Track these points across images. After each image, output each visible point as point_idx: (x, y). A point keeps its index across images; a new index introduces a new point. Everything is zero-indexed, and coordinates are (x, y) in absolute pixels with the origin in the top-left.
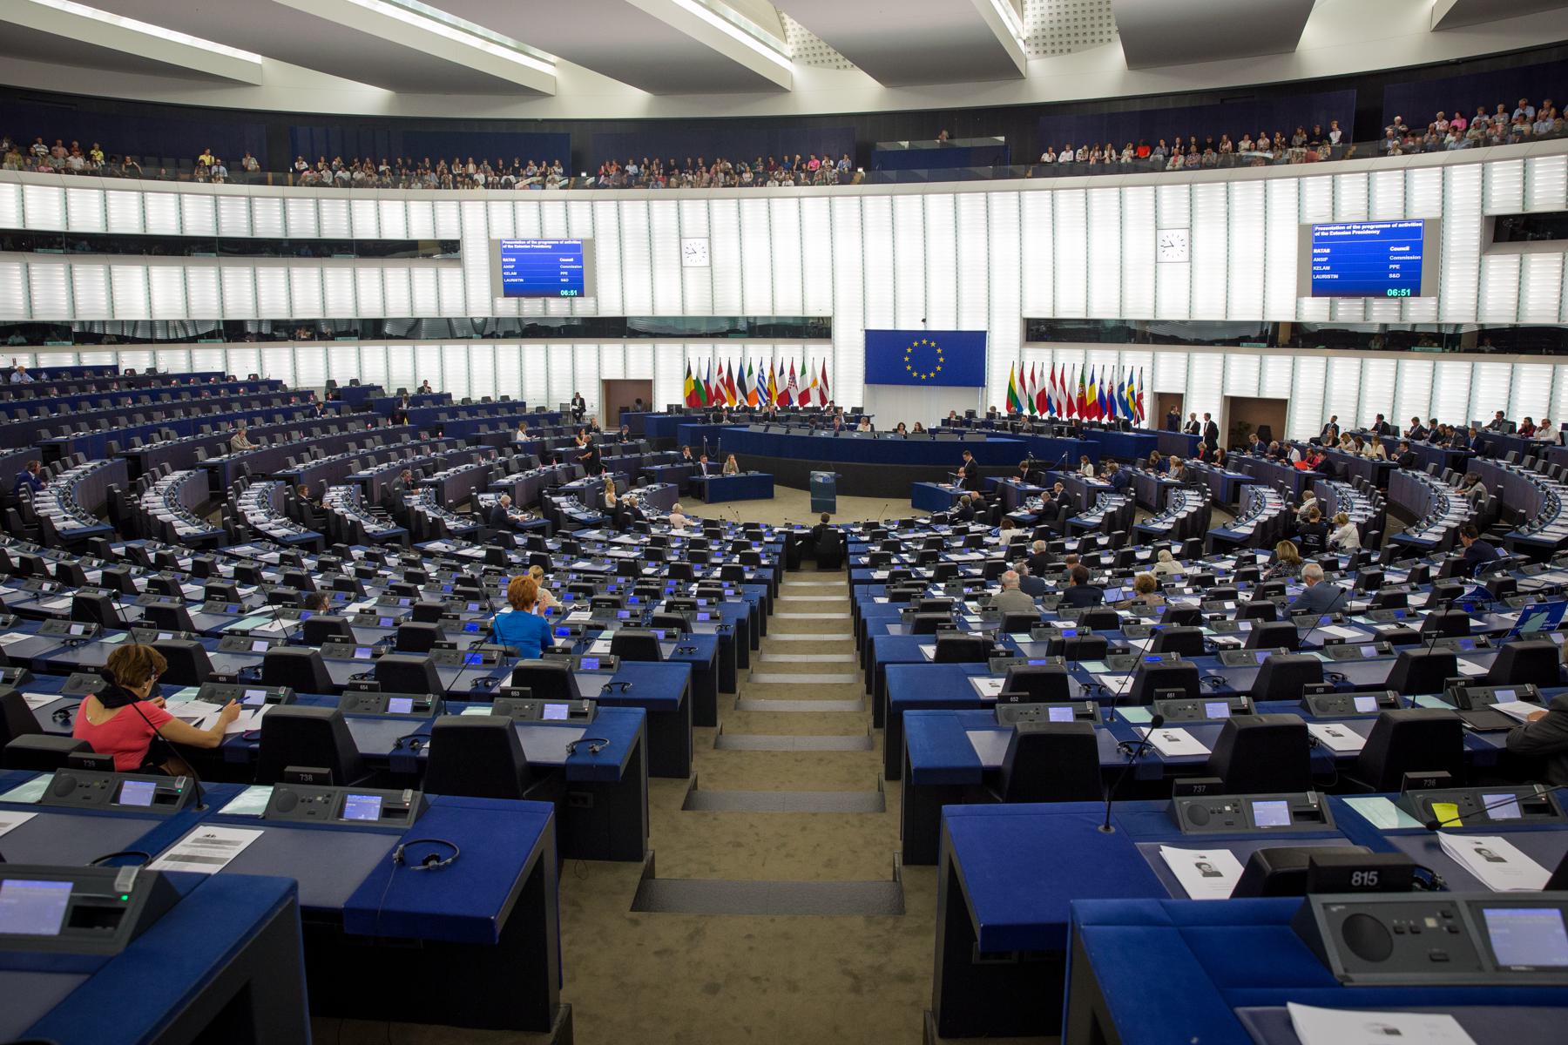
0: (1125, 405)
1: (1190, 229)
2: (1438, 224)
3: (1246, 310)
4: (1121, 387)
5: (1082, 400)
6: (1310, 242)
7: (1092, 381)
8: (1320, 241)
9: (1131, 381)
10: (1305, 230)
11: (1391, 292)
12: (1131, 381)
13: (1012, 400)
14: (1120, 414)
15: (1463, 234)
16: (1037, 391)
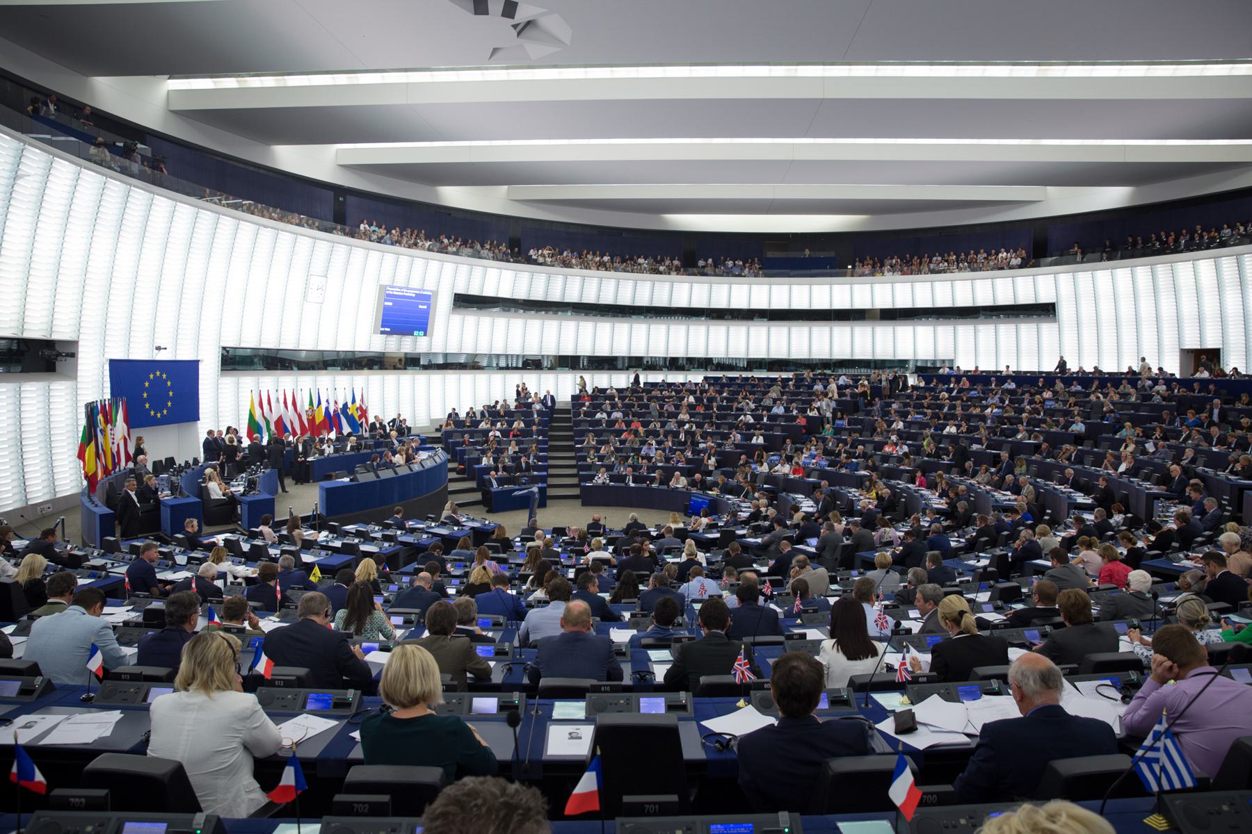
0: (351, 420)
1: (326, 276)
2: (436, 293)
3: (345, 344)
4: (345, 405)
5: (312, 421)
6: (383, 296)
7: (319, 403)
8: (389, 297)
9: (354, 401)
10: (383, 288)
11: (416, 333)
12: (354, 401)
13: (254, 428)
14: (347, 429)
15: (444, 302)
16: (274, 418)
